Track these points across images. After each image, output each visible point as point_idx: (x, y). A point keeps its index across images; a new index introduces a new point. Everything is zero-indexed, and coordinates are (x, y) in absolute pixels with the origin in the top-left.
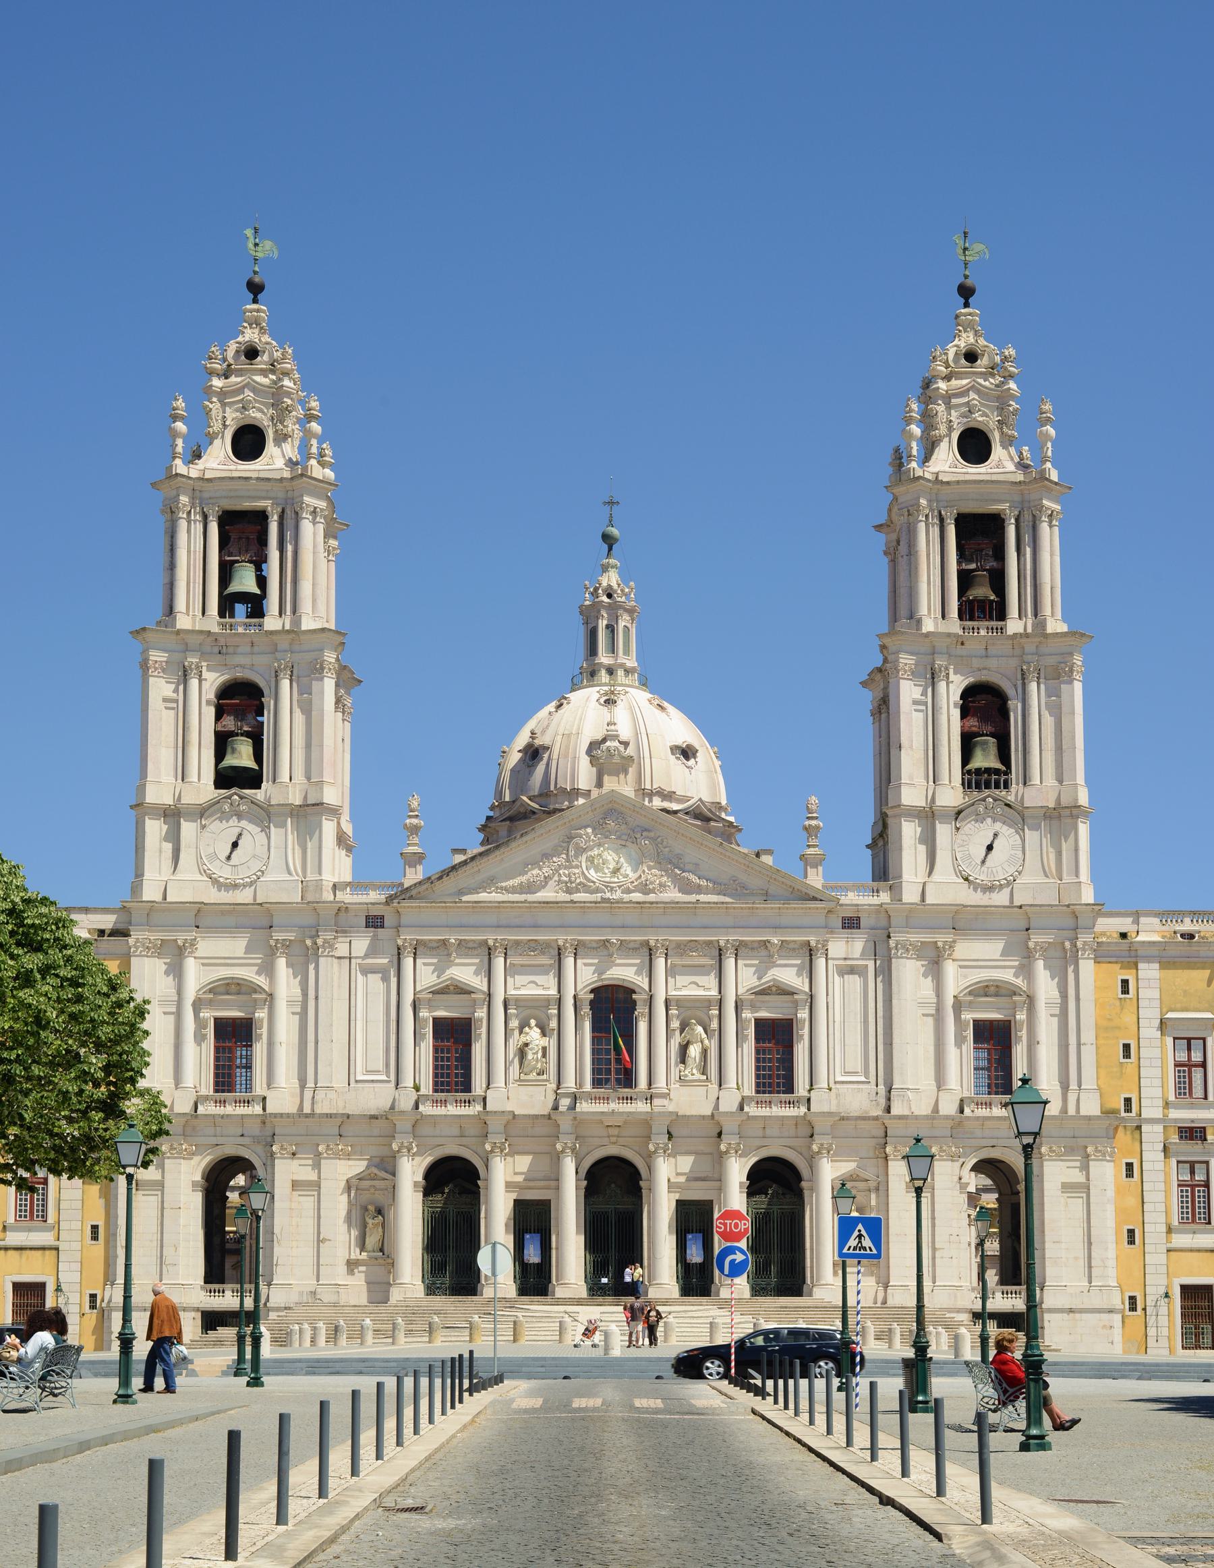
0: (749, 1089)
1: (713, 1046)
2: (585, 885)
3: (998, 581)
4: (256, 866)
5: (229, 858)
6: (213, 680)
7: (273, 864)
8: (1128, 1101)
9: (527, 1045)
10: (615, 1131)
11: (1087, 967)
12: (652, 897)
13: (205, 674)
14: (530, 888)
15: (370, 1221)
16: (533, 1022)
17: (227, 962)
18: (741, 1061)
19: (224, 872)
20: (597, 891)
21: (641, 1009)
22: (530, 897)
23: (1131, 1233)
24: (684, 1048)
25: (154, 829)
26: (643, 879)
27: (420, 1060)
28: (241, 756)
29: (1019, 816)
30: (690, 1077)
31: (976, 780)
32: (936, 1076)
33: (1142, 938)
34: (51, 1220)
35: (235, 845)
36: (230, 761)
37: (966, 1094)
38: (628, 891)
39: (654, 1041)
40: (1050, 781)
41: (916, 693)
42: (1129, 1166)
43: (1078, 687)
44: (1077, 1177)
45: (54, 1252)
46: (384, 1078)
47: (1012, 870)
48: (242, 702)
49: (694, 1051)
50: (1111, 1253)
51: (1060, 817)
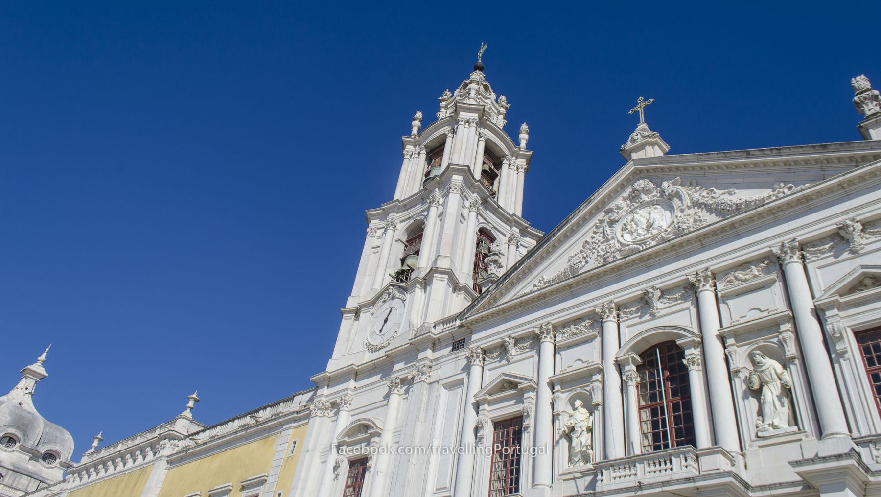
1: (794, 377)
5: (381, 330)
9: (572, 429)
16: (578, 403)
19: (377, 341)
21: (692, 353)
30: (771, 431)
35: (386, 321)
39: (714, 391)
49: (771, 393)
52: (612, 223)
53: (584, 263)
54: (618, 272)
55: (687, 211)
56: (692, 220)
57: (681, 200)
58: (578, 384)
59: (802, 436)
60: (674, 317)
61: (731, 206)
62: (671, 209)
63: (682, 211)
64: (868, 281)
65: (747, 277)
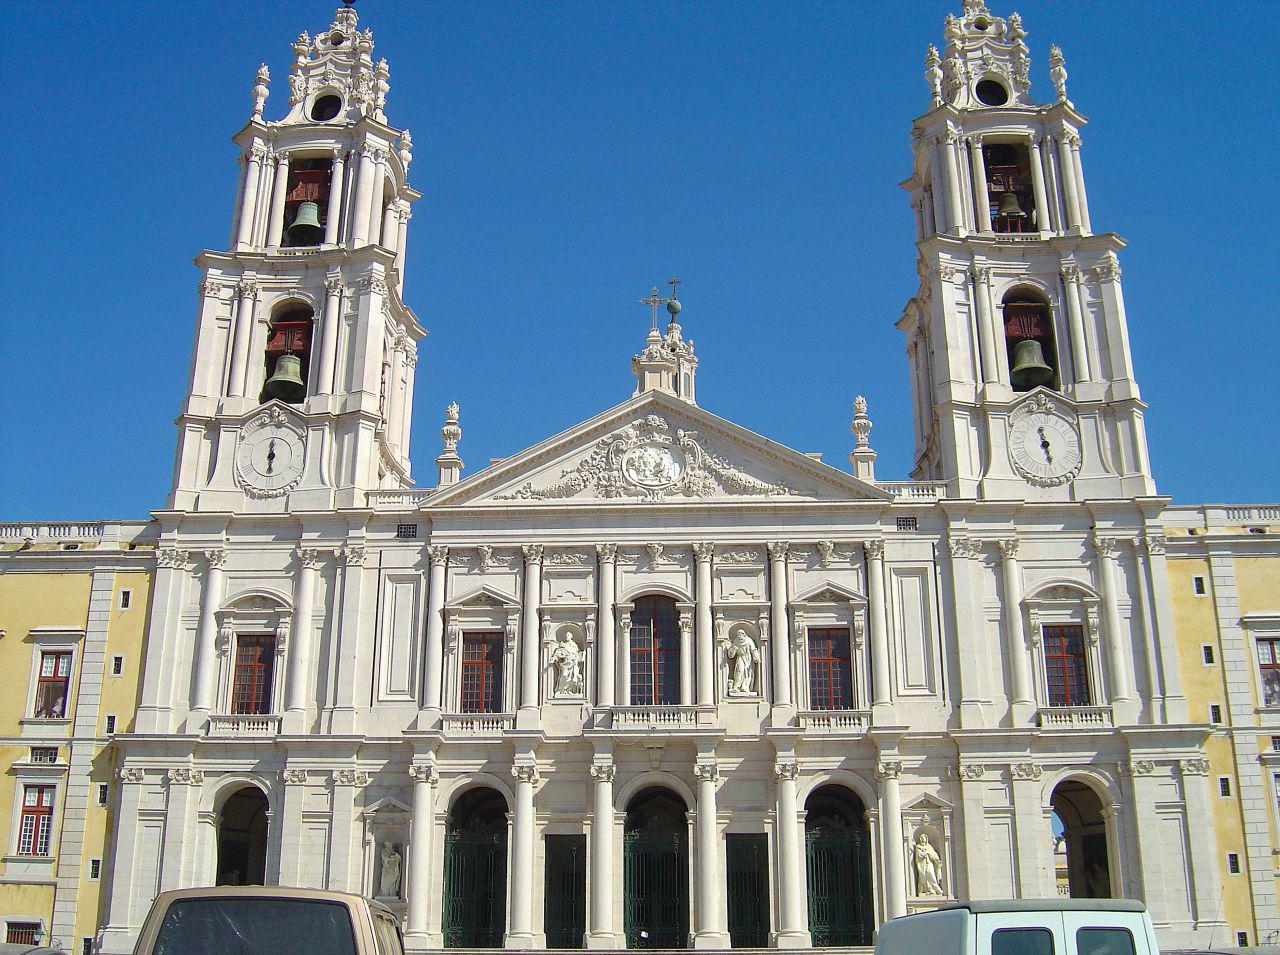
0: (804, 704)
1: (761, 656)
2: (625, 489)
3: (1028, 200)
4: (290, 477)
6: (268, 302)
7: (307, 472)
8: (1216, 709)
9: (562, 660)
10: (657, 754)
11: (1159, 563)
12: (695, 499)
13: (261, 295)
14: (568, 491)
15: (386, 860)
16: (569, 636)
17: (258, 574)
18: (794, 669)
19: (259, 483)
20: (637, 494)
22: (564, 500)
23: (1234, 858)
24: (732, 661)
25: (195, 444)
26: (686, 481)
27: (446, 673)
28: (291, 371)
29: (1073, 410)
31: (1022, 380)
32: (1002, 686)
33: (1211, 532)
34: (52, 852)
36: (278, 377)
37: (1041, 706)
38: (672, 494)
39: (702, 651)
40: (1098, 377)
41: (960, 296)
42: (1224, 781)
43: (1118, 287)
44: (1170, 794)
45: (52, 888)
46: (408, 698)
47: (1070, 467)
48: (294, 327)
49: (743, 664)
50: (1216, 884)
51: (1113, 411)
52: (619, 451)
53: (582, 487)
54: (624, 517)
55: (697, 472)
56: (701, 484)
57: (694, 456)
58: (576, 621)
59: (759, 700)
60: (671, 579)
61: (740, 486)
62: (683, 464)
63: (693, 469)
64: (828, 595)
65: (741, 559)
